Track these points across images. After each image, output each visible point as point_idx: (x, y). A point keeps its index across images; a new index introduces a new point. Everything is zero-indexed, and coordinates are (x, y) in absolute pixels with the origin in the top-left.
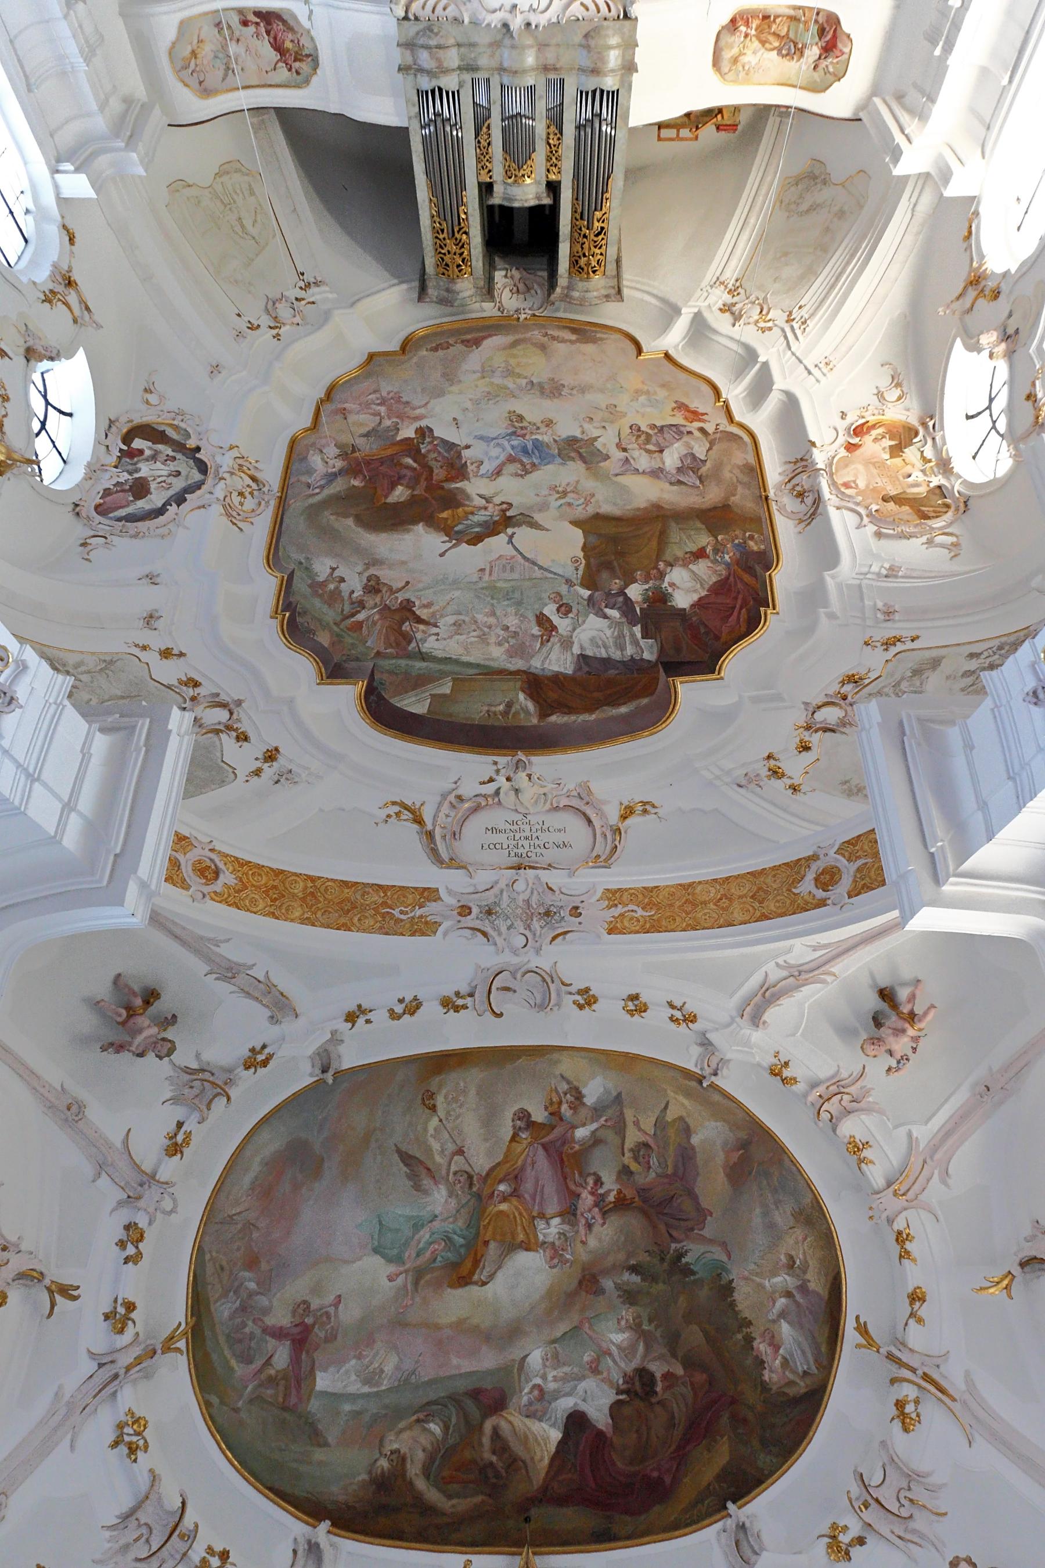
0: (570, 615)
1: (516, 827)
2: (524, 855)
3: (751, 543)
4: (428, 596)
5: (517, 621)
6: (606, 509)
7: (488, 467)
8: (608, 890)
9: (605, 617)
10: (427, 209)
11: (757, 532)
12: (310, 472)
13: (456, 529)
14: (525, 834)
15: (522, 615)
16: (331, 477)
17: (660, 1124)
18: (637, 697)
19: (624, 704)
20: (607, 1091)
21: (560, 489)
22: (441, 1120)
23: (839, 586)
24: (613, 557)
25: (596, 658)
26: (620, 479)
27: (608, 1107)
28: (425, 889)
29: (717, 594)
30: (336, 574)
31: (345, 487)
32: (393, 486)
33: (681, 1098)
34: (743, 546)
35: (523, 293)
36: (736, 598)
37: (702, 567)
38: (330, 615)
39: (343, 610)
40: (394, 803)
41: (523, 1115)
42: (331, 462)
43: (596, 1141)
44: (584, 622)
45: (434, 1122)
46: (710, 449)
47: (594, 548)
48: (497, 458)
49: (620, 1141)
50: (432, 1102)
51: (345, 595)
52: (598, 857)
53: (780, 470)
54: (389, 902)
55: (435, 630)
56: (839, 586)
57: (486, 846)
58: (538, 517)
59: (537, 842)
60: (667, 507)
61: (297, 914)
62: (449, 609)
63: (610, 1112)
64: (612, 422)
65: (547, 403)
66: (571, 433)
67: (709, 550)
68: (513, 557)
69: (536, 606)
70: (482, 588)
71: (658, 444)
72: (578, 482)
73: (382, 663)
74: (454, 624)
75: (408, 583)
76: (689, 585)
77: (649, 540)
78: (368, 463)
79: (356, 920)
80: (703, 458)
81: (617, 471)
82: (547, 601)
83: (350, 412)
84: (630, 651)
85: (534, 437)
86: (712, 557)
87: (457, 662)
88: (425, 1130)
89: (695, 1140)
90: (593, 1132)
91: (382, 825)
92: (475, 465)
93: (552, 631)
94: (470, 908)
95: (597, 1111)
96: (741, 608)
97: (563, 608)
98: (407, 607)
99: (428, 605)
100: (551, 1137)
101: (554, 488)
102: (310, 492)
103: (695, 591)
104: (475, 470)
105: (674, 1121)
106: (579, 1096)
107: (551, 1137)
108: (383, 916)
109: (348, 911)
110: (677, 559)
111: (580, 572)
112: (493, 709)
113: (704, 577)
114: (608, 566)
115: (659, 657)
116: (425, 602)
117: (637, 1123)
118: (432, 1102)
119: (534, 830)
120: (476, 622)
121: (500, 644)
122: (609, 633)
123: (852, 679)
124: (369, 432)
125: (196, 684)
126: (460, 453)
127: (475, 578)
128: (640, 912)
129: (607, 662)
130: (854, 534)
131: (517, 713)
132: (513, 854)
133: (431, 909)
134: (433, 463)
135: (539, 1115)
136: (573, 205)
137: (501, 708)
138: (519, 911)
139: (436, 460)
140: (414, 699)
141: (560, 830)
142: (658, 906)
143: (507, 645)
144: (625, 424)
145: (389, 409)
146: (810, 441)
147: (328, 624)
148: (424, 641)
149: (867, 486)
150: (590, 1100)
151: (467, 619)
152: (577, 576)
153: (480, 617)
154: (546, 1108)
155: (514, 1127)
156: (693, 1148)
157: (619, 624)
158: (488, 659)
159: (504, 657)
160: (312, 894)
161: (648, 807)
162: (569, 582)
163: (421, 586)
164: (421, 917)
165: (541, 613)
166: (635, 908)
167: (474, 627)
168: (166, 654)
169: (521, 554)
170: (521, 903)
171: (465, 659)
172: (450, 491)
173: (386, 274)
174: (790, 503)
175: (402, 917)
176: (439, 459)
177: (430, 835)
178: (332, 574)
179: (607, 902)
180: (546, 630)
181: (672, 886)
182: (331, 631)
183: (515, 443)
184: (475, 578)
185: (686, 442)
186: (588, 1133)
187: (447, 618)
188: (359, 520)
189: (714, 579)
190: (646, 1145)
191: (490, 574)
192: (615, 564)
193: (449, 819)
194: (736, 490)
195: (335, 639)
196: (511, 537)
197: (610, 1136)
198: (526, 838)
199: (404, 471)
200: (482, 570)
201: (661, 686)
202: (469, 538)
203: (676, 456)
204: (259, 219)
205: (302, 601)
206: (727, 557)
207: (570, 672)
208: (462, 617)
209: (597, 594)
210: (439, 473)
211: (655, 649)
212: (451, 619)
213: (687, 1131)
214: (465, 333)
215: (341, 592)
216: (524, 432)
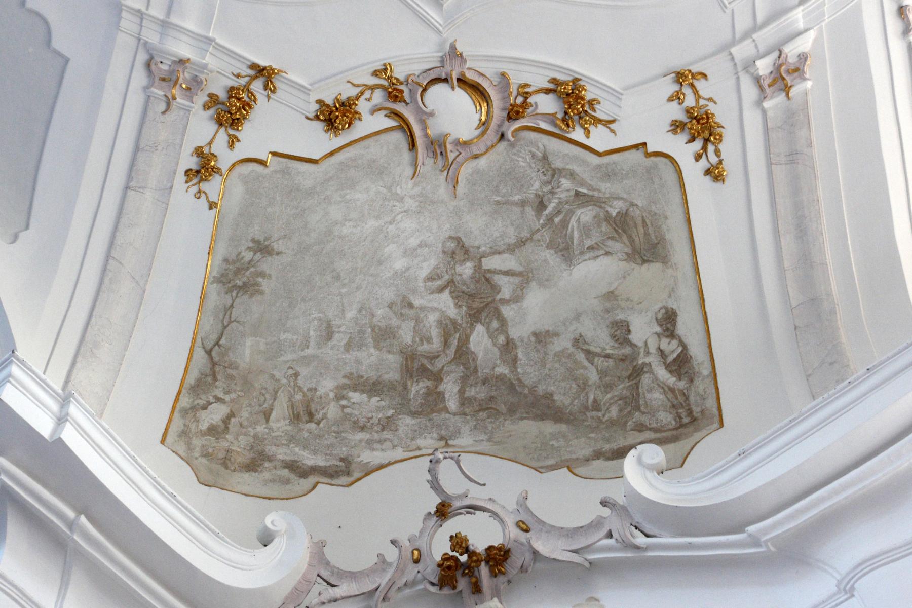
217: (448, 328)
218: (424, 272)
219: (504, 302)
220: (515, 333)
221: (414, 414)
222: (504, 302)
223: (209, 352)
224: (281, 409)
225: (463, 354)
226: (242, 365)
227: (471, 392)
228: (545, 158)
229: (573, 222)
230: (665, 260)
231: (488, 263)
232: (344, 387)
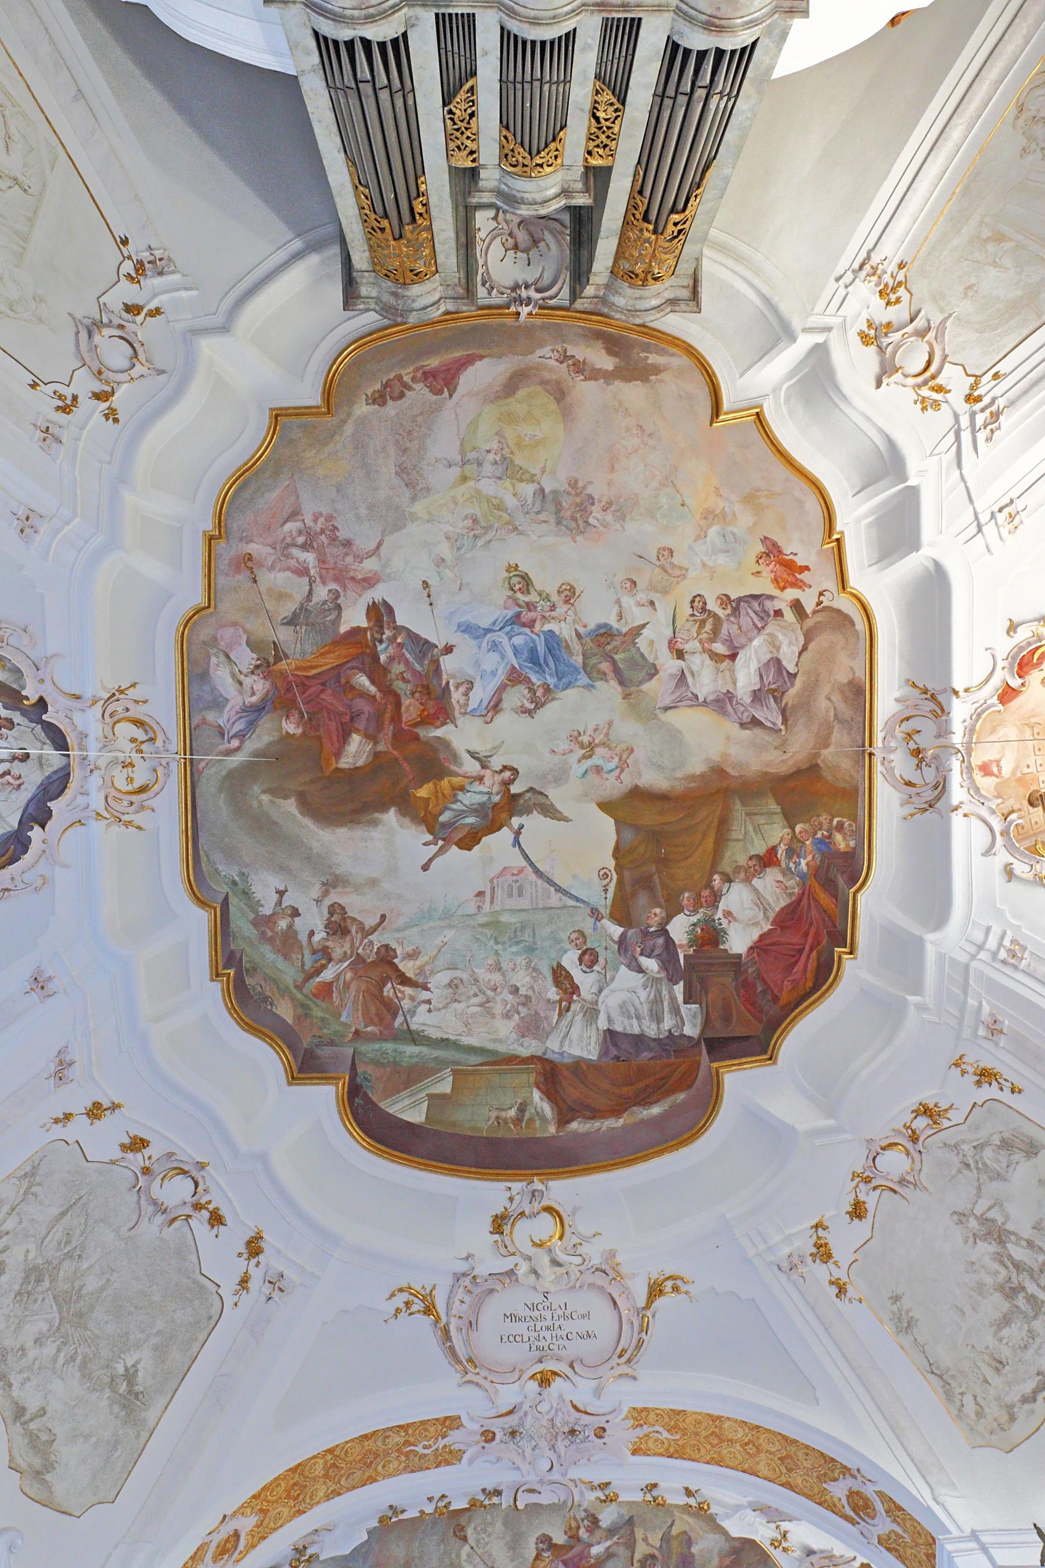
0: (596, 968)
1: (536, 1313)
2: (546, 1348)
3: (838, 837)
4: (413, 938)
5: (528, 979)
6: (652, 779)
7: (480, 695)
8: (634, 1409)
9: (640, 970)
10: (352, 200)
11: (849, 819)
12: (218, 703)
13: (442, 819)
14: (545, 1324)
15: (535, 969)
16: (255, 712)
17: (666, 1538)
18: (673, 1091)
19: (656, 1102)
20: (621, 1516)
21: (585, 739)
22: (472, 1548)
23: (941, 957)
24: (653, 868)
25: (626, 1035)
26: (671, 717)
27: (621, 1528)
28: (446, 1418)
29: (783, 928)
30: (287, 901)
31: (275, 736)
32: (344, 738)
33: (686, 1517)
34: (826, 842)
35: (526, 251)
36: (806, 935)
37: (769, 883)
38: (289, 973)
39: (303, 964)
40: (401, 1290)
41: (546, 1540)
42: (248, 681)
43: (609, 1555)
44: (613, 979)
45: (466, 1549)
46: (805, 648)
47: (631, 850)
48: (494, 674)
49: (630, 1554)
50: (463, 1534)
51: (303, 937)
53: (897, 694)
54: (412, 1439)
55: (425, 995)
56: (941, 957)
57: (505, 1339)
58: (555, 795)
59: (559, 1332)
60: (733, 772)
61: (321, 1494)
62: (442, 961)
63: (622, 1531)
64: (665, 592)
65: (566, 546)
66: (602, 620)
67: (781, 852)
68: (521, 870)
69: (553, 955)
70: (482, 925)
71: (729, 642)
72: (610, 724)
73: (365, 1048)
74: (449, 985)
75: (383, 917)
76: (749, 914)
77: (704, 835)
78: (303, 684)
79: (380, 1468)
80: (792, 669)
81: (667, 701)
82: (568, 946)
83: (260, 565)
84: (668, 1023)
85: (547, 627)
86: (783, 865)
87: (456, 1045)
88: (458, 1556)
89: (695, 1550)
90: (608, 1548)
91: (392, 1321)
92: (462, 689)
93: (573, 993)
94: (494, 1434)
95: (611, 1532)
96: (811, 950)
97: (587, 957)
98: (386, 957)
99: (413, 955)
100: (570, 1554)
101: (575, 738)
102: (225, 746)
103: (756, 924)
104: (462, 700)
105: (678, 1534)
106: (595, 1521)
107: (570, 1554)
108: (407, 1455)
109: (371, 1462)
110: (737, 869)
111: (610, 895)
112: (503, 1114)
113: (770, 900)
114: (645, 883)
115: (703, 1032)
116: (409, 949)
117: (645, 1540)
118: (463, 1534)
119: (556, 1317)
120: (476, 980)
121: (507, 1016)
122: (643, 995)
123: (925, 1111)
124: (295, 614)
125: (144, 1143)
126: (438, 661)
127: (471, 909)
128: (665, 1434)
129: (639, 1039)
130: (977, 859)
131: (531, 1120)
132: (534, 1348)
133: (454, 1438)
134: (400, 686)
135: (560, 1538)
136: (631, 197)
137: (512, 1113)
138: (544, 1431)
139: (404, 680)
140: (407, 1102)
141: (583, 1317)
142: (684, 1432)
143: (516, 1017)
144: (685, 592)
145: (322, 561)
146: (954, 690)
147: (287, 987)
148: (413, 1013)
149: (1014, 773)
150: (604, 1524)
151: (465, 976)
152: (604, 902)
153: (481, 973)
154: (566, 1533)
155: (537, 1549)
156: (693, 1556)
157: (657, 981)
158: (495, 1041)
159: (514, 1036)
160: (334, 1465)
161: (679, 1282)
162: (595, 913)
163: (401, 922)
164: (445, 1446)
165: (559, 965)
166: (661, 1429)
167: (475, 989)
168: (95, 1112)
169: (531, 864)
170: (545, 1422)
171: (466, 1040)
172: (427, 743)
173: (280, 226)
174: (901, 764)
175: (426, 1451)
176: (408, 676)
177: (446, 1332)
178: (279, 903)
179: (632, 1421)
180: (565, 991)
181: (700, 1414)
182: (293, 999)
183: (518, 640)
184: (471, 909)
185: (771, 635)
186: (602, 1550)
187: (439, 976)
188: (307, 806)
189: (783, 904)
190: (653, 1557)
191: (492, 902)
192: (656, 879)
193: (465, 1307)
194: (830, 734)
195: (300, 1011)
196: (518, 833)
197: (622, 1551)
198: (548, 1328)
199: (360, 704)
200: (480, 894)
201: (702, 1074)
202: (461, 835)
203: (754, 666)
204: (13, 130)
205: (248, 950)
206: (803, 862)
207: (595, 1058)
208: (457, 974)
209: (631, 932)
210: (411, 708)
211: (699, 1021)
212: (444, 977)
213: (689, 1542)
214: (430, 352)
215: (296, 933)
216: (531, 615)
219: (1004, 1224)
222: (1004, 1224)
228: (945, 1144)
229: (987, 1161)
231: (978, 1211)
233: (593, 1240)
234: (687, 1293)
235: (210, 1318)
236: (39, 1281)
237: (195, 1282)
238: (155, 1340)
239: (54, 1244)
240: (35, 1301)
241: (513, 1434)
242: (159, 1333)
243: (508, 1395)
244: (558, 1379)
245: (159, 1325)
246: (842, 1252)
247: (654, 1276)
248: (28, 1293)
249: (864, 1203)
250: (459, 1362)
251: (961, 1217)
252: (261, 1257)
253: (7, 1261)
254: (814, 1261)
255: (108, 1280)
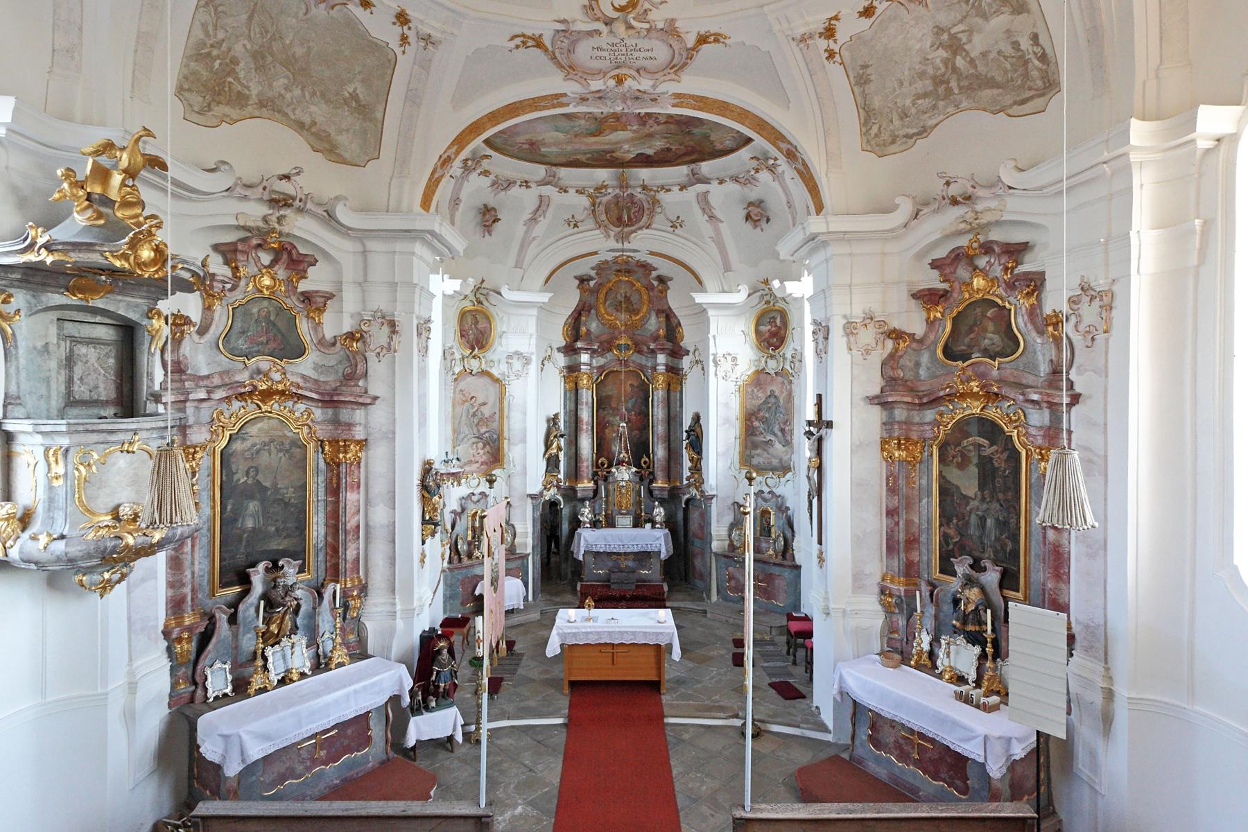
1: (615, 48)
52: (674, 66)
141: (648, 50)
198: (623, 55)
217: (945, 62)
218: (929, 44)
219: (964, 44)
220: (972, 55)
221: (943, 100)
222: (964, 44)
223: (864, 109)
224: (895, 117)
225: (955, 69)
226: (877, 108)
227: (962, 84)
230: (1028, 11)
231: (953, 31)
232: (914, 100)
233: (660, 7)
234: (723, 43)
235: (390, 60)
236: (263, 58)
237: (369, 41)
238: (359, 77)
239: (258, 36)
240: (270, 69)
241: (600, 98)
242: (359, 73)
243: (596, 85)
244: (629, 79)
245: (357, 69)
246: (842, 35)
247: (702, 32)
248: (263, 66)
249: (876, 8)
250: (564, 68)
251: (939, 30)
252: (410, 25)
253: (236, 55)
254: (820, 37)
255: (309, 47)
